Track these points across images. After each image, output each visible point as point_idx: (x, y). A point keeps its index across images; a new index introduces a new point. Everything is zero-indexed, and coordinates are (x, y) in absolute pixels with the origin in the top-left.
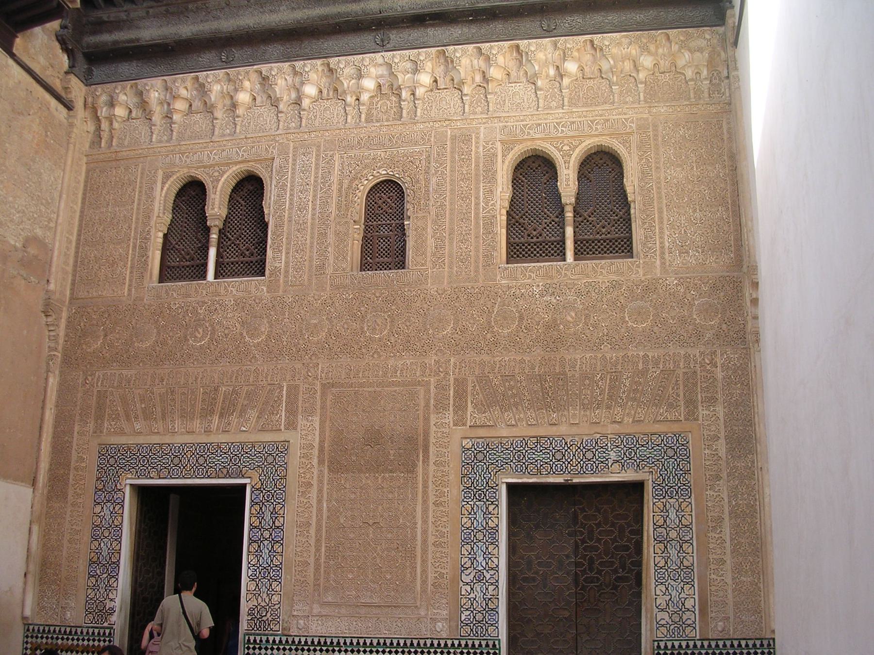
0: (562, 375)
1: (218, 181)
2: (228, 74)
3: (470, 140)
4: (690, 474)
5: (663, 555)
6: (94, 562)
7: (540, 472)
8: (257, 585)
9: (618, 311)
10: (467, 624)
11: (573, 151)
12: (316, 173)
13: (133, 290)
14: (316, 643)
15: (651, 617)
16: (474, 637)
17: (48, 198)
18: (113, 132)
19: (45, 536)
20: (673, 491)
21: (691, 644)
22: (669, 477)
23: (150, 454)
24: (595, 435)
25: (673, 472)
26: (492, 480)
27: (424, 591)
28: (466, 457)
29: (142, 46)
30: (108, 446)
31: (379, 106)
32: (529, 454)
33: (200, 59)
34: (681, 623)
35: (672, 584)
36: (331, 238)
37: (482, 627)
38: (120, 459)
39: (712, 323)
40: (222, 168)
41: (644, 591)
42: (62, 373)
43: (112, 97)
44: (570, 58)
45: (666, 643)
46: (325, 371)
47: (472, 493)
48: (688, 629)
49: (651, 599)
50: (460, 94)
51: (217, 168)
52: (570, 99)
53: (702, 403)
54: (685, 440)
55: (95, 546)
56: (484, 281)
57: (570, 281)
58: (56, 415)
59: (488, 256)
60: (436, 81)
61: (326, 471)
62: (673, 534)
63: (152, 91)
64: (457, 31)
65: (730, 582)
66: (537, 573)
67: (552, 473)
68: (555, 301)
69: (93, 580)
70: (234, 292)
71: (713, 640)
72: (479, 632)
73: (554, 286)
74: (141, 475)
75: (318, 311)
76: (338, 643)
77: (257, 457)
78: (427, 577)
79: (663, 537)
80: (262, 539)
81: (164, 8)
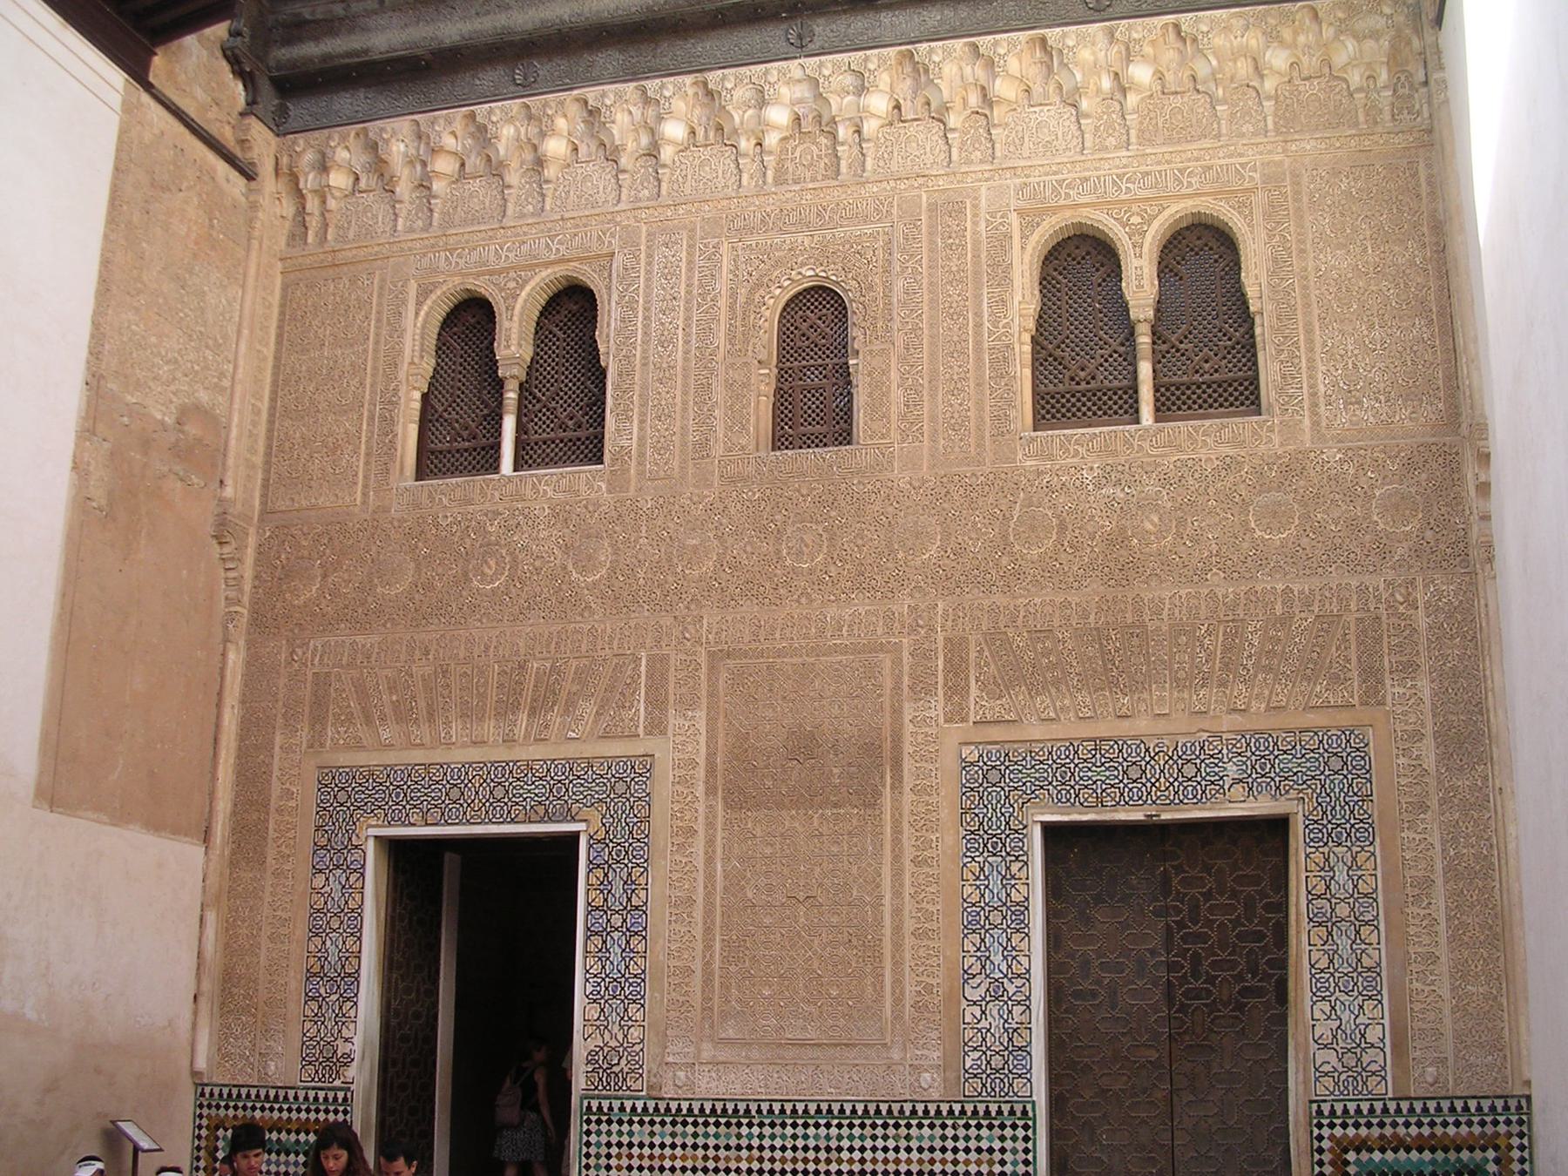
0: (1138, 627)
1: (515, 297)
2: (528, 107)
3: (962, 211)
4: (1371, 801)
5: (1326, 947)
6: (315, 975)
7: (1102, 802)
8: (602, 1010)
9: (1236, 510)
11: (1149, 225)
12: (689, 278)
13: (372, 493)
14: (708, 1112)
16: (989, 1098)
17: (218, 337)
18: (327, 215)
19: (228, 929)
20: (1341, 833)
21: (1378, 1106)
22: (1333, 808)
23: (409, 783)
24: (1198, 734)
25: (1341, 799)
26: (1016, 818)
27: (898, 1017)
28: (968, 777)
29: (374, 63)
30: (334, 771)
31: (797, 154)
32: (1081, 770)
33: (478, 82)
34: (1359, 1069)
35: (1342, 999)
36: (719, 393)
37: (1002, 1080)
38: (357, 792)
39: (1407, 529)
40: (523, 273)
41: (1292, 1012)
42: (250, 644)
43: (323, 155)
44: (1139, 58)
45: (1332, 1106)
46: (714, 631)
47: (981, 841)
49: (1305, 1027)
50: (943, 128)
51: (512, 274)
52: (1141, 131)
53: (1391, 673)
54: (1362, 741)
55: (316, 947)
57: (1149, 460)
59: (1001, 419)
60: (898, 107)
62: (1343, 910)
63: (393, 140)
65: (1446, 993)
66: (1098, 982)
67: (1122, 803)
68: (1122, 496)
69: (314, 1005)
70: (550, 493)
71: (1416, 1099)
72: (997, 1090)
73: (1120, 468)
74: (393, 819)
75: (699, 523)
76: (747, 1111)
78: (902, 993)
79: (1324, 915)
80: (609, 930)
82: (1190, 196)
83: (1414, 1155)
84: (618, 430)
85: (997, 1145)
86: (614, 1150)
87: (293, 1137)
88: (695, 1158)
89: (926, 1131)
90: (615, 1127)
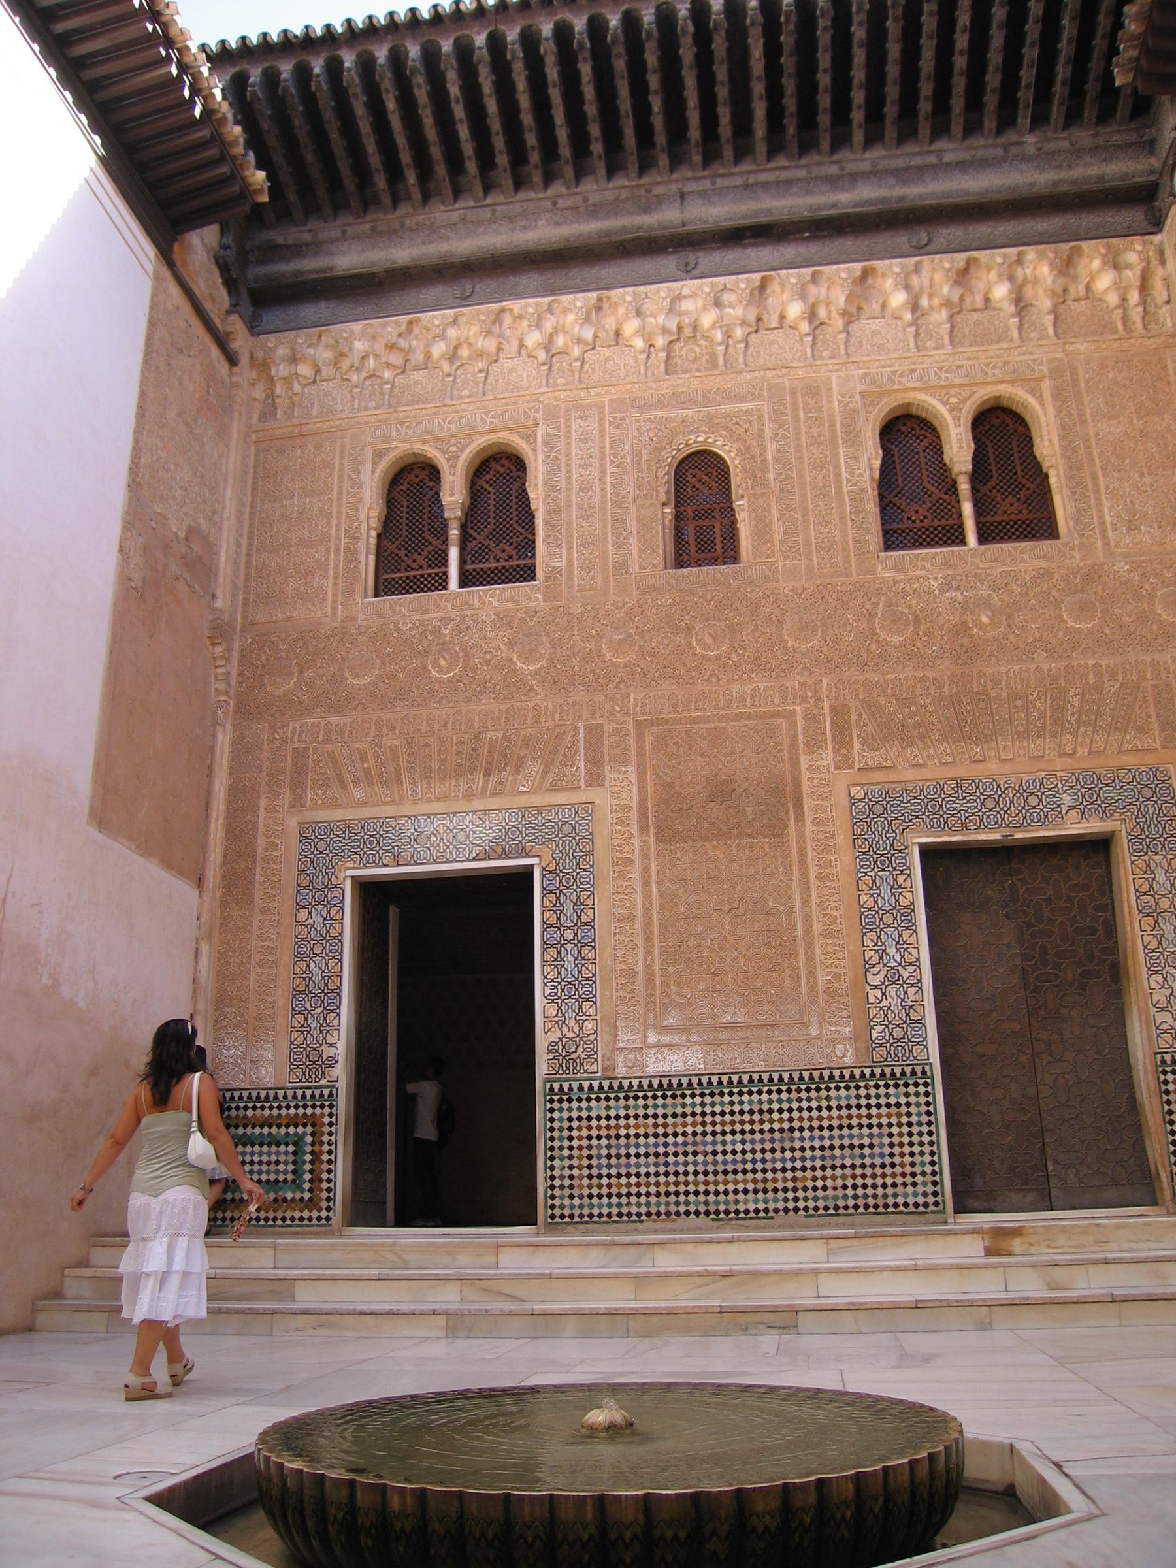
6: (301, 992)
8: (560, 1008)
10: (881, 1045)
14: (656, 1087)
15: (1147, 1022)
19: (222, 960)
31: (684, 352)
36: (633, 526)
42: (235, 727)
43: (293, 350)
51: (453, 441)
56: (858, 575)
58: (230, 786)
61: (652, 841)
64: (789, 251)
69: (301, 1018)
76: (690, 1084)
78: (816, 982)
81: (368, 226)
85: (903, 1100)
86: (575, 1124)
88: (646, 1126)
89: (843, 1092)
90: (575, 1104)
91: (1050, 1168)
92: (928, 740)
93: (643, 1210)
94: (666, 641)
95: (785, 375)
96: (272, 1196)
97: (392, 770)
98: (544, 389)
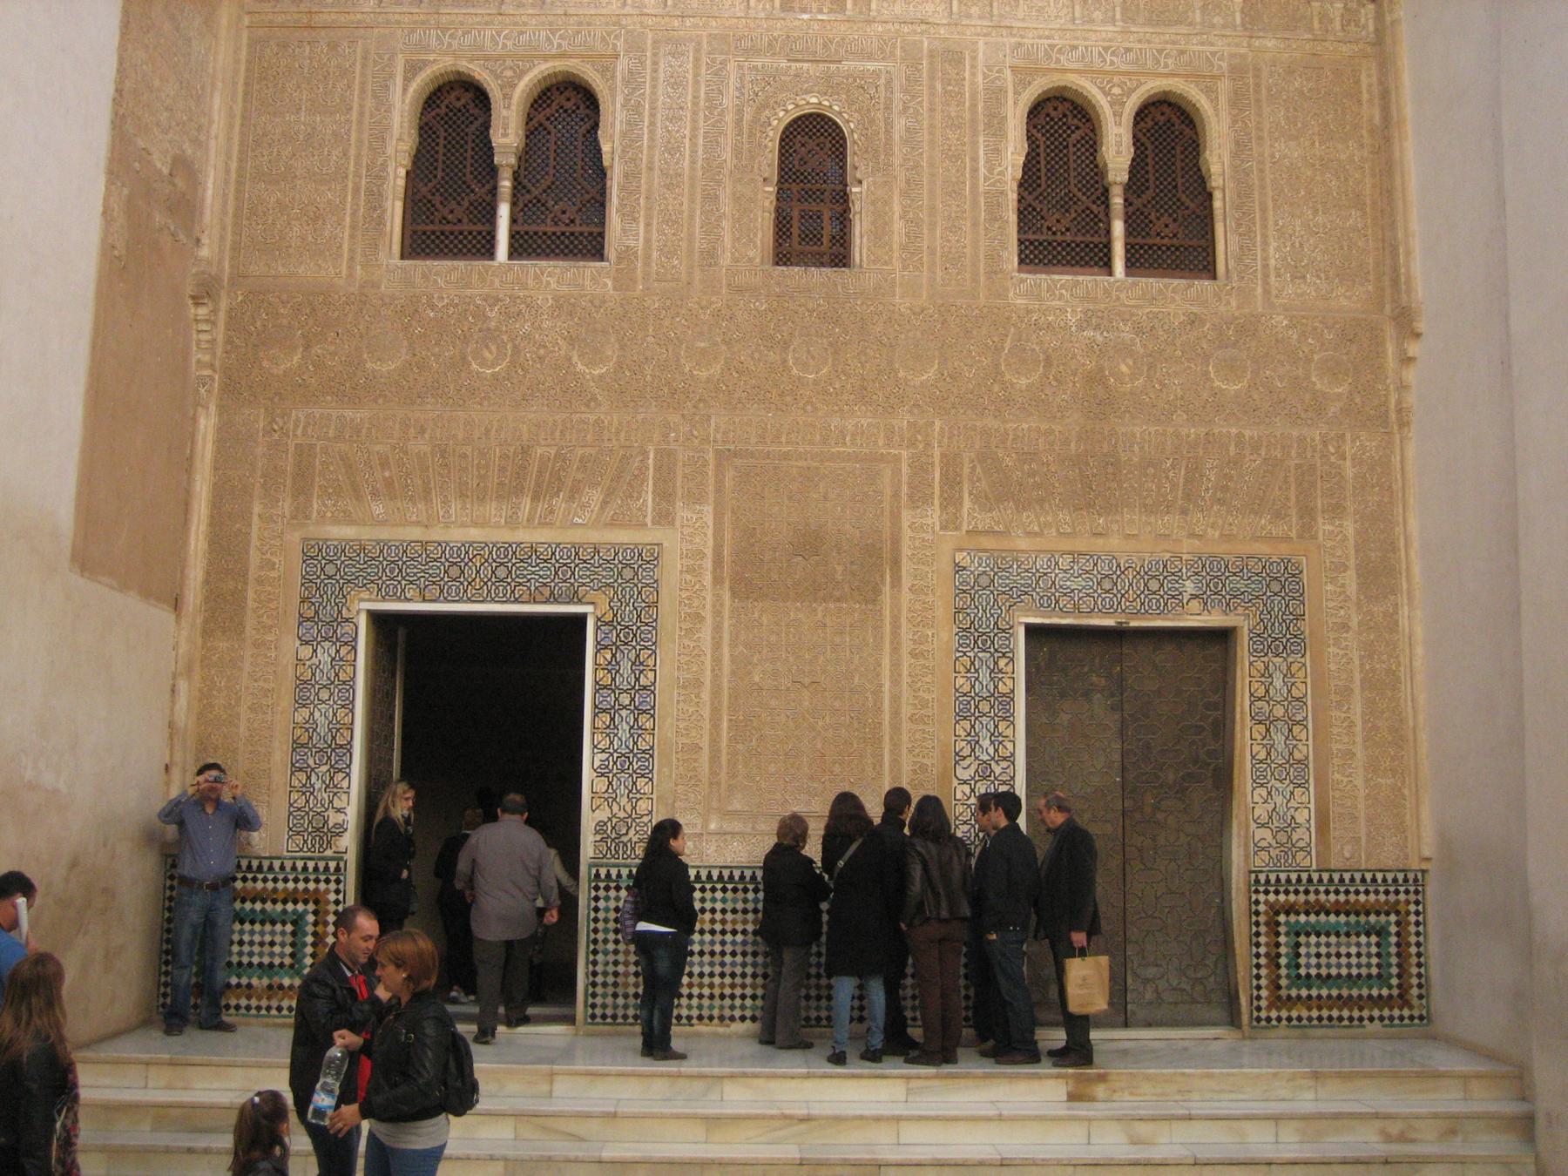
5: (1265, 742)
8: (610, 783)
14: (715, 878)
15: (1246, 837)
21: (1304, 876)
22: (1273, 624)
36: (726, 206)
42: (222, 409)
48: (1301, 855)
51: (509, 63)
59: (994, 258)
61: (727, 596)
62: (1279, 711)
65: (1359, 782)
69: (303, 777)
70: (554, 286)
73: (1100, 314)
77: (604, 569)
82: (1167, 75)
83: (1332, 918)
84: (624, 231)
87: (279, 907)
91: (1129, 981)
92: (1047, 506)
93: (695, 1013)
94: (757, 355)
95: (922, 33)
96: (266, 981)
97: (420, 482)
98: (628, 10)
